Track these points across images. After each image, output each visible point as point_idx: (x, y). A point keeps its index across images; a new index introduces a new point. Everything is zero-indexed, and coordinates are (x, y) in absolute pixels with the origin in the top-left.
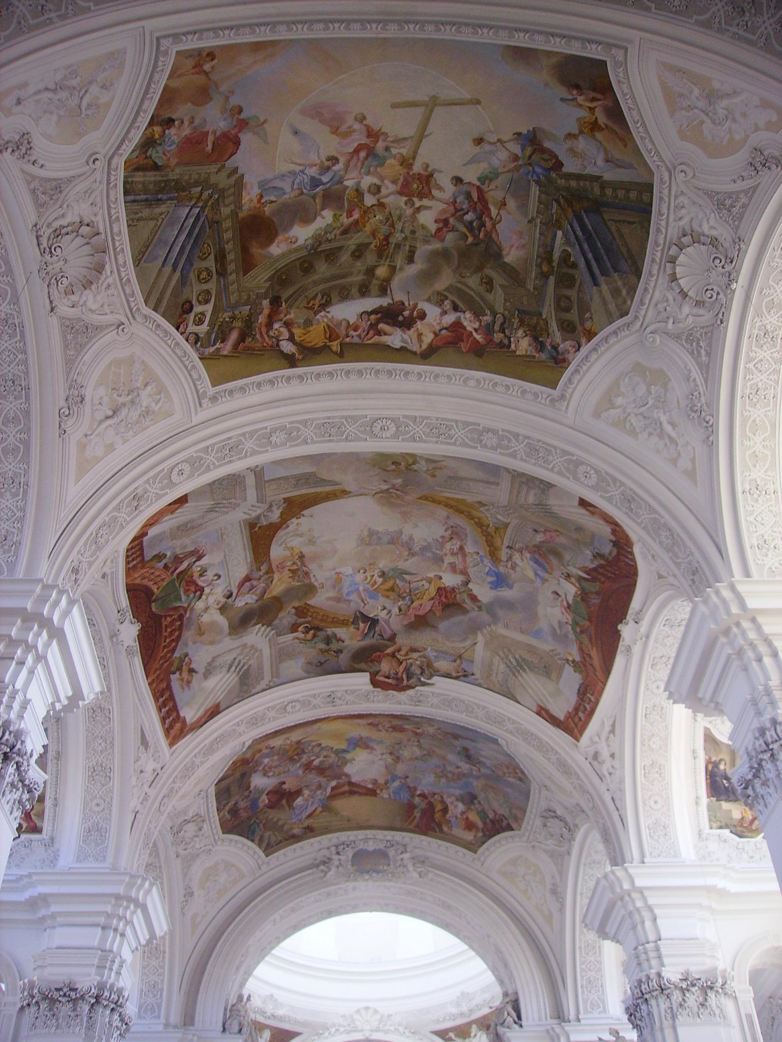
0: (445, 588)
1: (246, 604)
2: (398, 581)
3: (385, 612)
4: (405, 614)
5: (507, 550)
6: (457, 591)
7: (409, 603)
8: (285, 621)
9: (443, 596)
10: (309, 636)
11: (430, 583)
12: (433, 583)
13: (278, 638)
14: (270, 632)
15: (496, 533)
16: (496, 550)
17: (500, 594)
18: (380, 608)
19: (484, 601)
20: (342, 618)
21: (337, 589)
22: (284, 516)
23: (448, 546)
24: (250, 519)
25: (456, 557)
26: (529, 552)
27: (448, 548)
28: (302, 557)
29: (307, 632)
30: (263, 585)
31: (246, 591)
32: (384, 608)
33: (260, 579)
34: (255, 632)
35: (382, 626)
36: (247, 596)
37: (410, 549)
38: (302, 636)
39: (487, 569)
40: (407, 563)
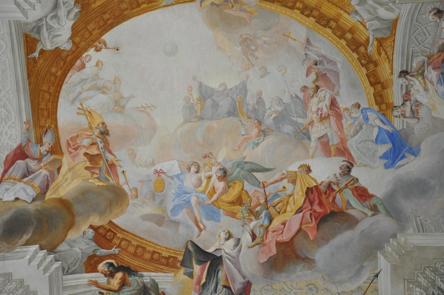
0: (316, 187)
1: (17, 199)
2: (248, 187)
3: (231, 242)
4: (262, 244)
5: (402, 81)
6: (335, 187)
7: (266, 223)
8: (77, 249)
9: (317, 201)
10: (115, 282)
11: (294, 182)
12: (298, 182)
13: (65, 277)
14: (51, 263)
15: (380, 54)
16: (384, 87)
17: (402, 171)
18: (223, 236)
19: (379, 196)
20: (165, 254)
21: (158, 201)
22: (77, 40)
23: (314, 104)
24: (26, 24)
25: (326, 124)
26: (434, 68)
27: (314, 109)
28: (105, 133)
29: (111, 275)
30: (44, 172)
31: (18, 177)
32: (230, 236)
33: (40, 160)
34: (28, 257)
35: (229, 268)
36: (20, 185)
37: (260, 123)
38: (103, 280)
39: (376, 132)
40: (259, 149)
